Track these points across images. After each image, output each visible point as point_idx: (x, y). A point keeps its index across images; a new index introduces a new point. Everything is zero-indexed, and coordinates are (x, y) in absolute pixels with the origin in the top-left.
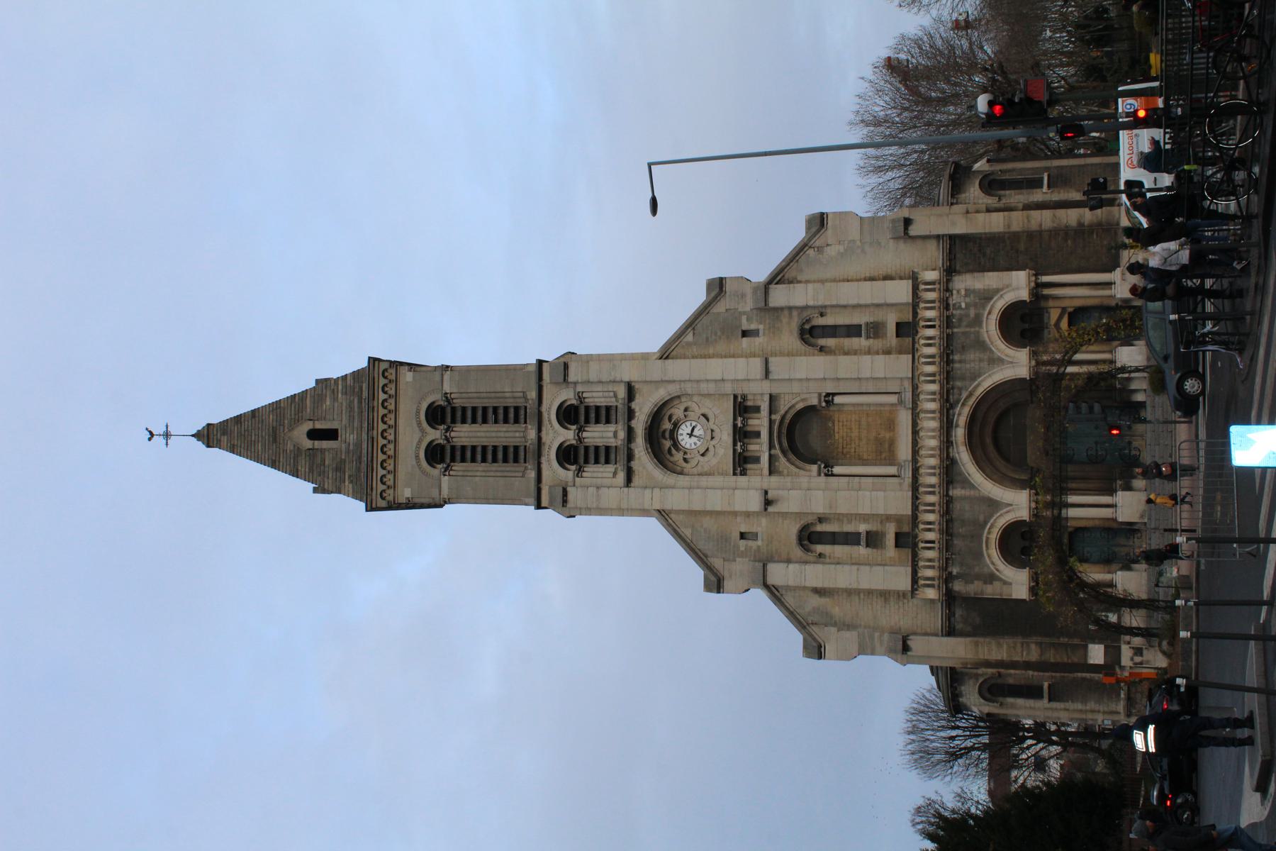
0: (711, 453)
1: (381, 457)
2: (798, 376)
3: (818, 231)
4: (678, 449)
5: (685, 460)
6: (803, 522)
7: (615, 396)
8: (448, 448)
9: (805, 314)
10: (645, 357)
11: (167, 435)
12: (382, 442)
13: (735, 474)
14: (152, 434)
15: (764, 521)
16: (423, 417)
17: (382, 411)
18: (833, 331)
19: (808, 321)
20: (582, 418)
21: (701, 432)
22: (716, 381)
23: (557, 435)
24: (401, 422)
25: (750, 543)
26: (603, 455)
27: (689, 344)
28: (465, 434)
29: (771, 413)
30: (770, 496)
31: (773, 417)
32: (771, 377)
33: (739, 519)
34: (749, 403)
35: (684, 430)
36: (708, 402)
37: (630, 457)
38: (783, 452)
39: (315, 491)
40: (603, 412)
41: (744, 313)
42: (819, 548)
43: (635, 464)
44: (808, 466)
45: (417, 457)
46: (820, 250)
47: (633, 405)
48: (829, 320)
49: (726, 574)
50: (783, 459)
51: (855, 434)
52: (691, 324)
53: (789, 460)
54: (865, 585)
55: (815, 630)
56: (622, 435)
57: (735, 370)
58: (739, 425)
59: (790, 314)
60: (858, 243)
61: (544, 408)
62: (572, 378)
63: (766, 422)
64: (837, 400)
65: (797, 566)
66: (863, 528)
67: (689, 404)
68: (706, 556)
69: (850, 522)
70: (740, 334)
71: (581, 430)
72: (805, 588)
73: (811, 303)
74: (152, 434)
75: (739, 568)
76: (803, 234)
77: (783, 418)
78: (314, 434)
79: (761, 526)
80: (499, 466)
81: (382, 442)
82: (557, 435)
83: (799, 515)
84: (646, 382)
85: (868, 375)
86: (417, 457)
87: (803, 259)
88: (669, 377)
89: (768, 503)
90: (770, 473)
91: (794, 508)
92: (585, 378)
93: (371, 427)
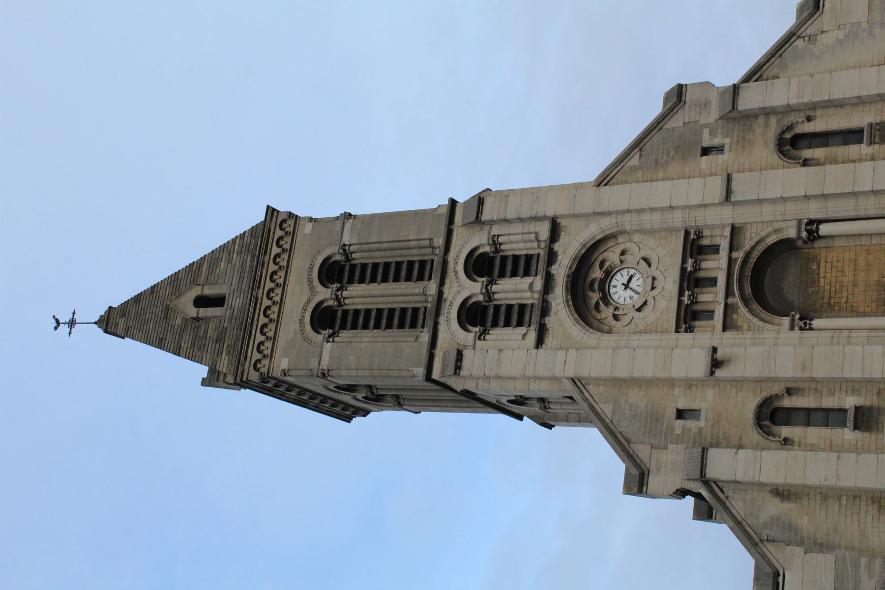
0: (647, 310)
1: (263, 320)
2: (769, 195)
3: (811, 15)
4: (607, 304)
5: (616, 317)
6: (765, 394)
7: (537, 239)
8: (340, 314)
9: (788, 120)
10: (578, 187)
11: (72, 323)
12: (266, 302)
13: (677, 331)
14: (57, 321)
15: (711, 393)
16: (315, 273)
17: (272, 267)
18: (824, 138)
19: (790, 128)
20: (496, 271)
21: (640, 282)
22: (662, 209)
23: (462, 288)
24: (291, 280)
25: (689, 423)
26: (515, 316)
27: (634, 169)
28: (359, 295)
29: (731, 249)
30: (719, 355)
31: (735, 255)
32: (733, 199)
33: (677, 391)
34: (705, 242)
35: (619, 280)
36: (651, 242)
37: (545, 310)
38: (745, 301)
39: (205, 382)
40: (522, 263)
41: (707, 125)
42: (785, 431)
43: (549, 321)
44: (777, 319)
45: (302, 320)
46: (812, 39)
47: (557, 247)
48: (818, 126)
49: (653, 467)
50: (743, 310)
51: (848, 278)
52: (638, 144)
53: (751, 311)
54: (847, 482)
55: (770, 550)
56: (539, 284)
57: (689, 193)
58: (689, 268)
59: (767, 125)
60: (865, 25)
61: (451, 258)
62: (486, 216)
63: (724, 264)
64: (824, 229)
65: (750, 452)
66: (850, 402)
67: (628, 245)
68: (628, 441)
69: (832, 393)
70: (699, 152)
71: (491, 282)
72: (762, 485)
73: (794, 101)
74: (57, 321)
75: (670, 463)
76: (794, 21)
77: (748, 255)
78: (201, 302)
79: (705, 400)
80: (395, 332)
81: (266, 302)
82: (462, 288)
83: (760, 381)
84: (574, 216)
85: (868, 188)
86: (302, 320)
87: (788, 52)
88: (604, 207)
89: (716, 364)
90: (725, 328)
91: (752, 371)
92: (502, 216)
93: (256, 284)
